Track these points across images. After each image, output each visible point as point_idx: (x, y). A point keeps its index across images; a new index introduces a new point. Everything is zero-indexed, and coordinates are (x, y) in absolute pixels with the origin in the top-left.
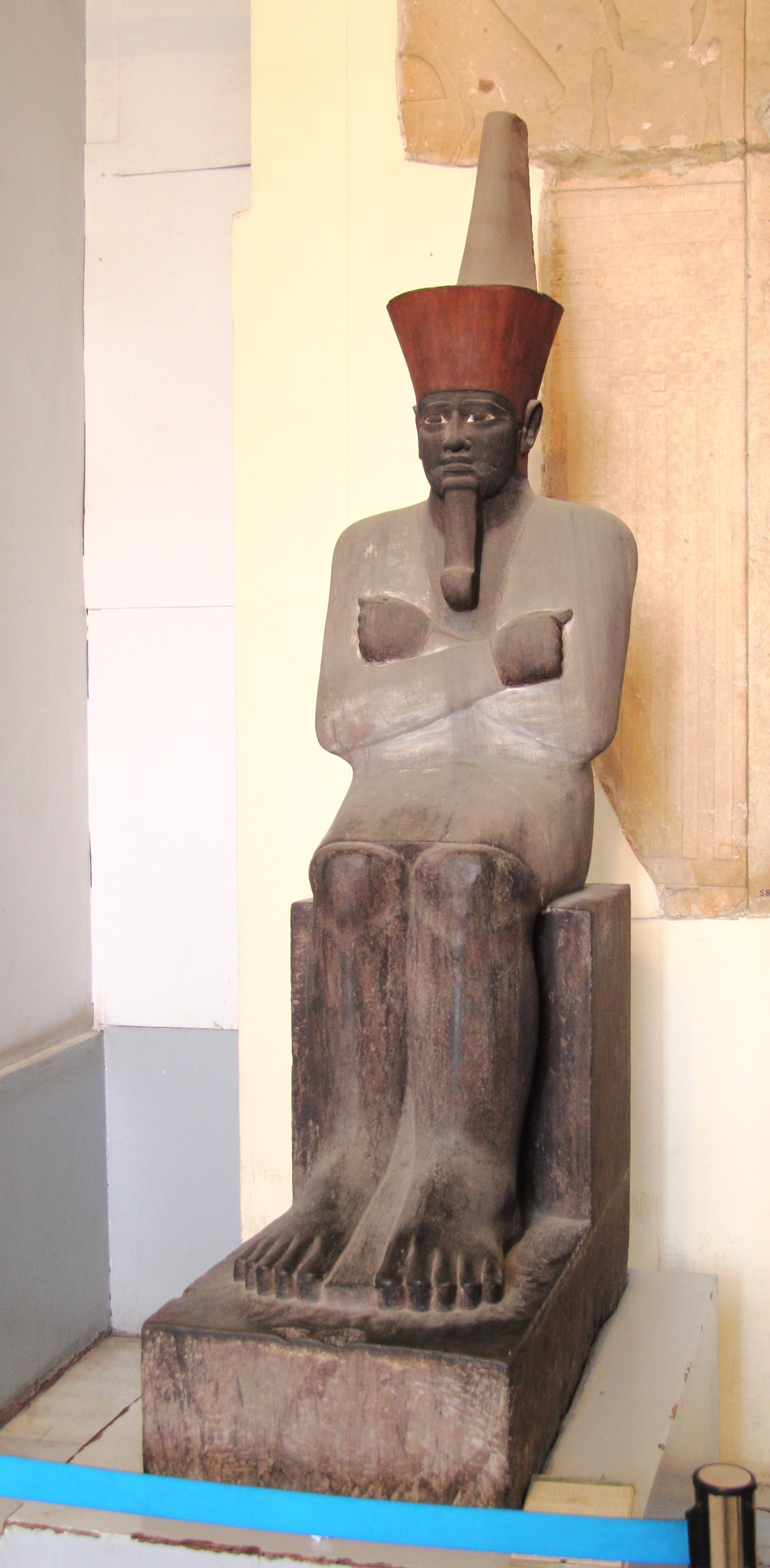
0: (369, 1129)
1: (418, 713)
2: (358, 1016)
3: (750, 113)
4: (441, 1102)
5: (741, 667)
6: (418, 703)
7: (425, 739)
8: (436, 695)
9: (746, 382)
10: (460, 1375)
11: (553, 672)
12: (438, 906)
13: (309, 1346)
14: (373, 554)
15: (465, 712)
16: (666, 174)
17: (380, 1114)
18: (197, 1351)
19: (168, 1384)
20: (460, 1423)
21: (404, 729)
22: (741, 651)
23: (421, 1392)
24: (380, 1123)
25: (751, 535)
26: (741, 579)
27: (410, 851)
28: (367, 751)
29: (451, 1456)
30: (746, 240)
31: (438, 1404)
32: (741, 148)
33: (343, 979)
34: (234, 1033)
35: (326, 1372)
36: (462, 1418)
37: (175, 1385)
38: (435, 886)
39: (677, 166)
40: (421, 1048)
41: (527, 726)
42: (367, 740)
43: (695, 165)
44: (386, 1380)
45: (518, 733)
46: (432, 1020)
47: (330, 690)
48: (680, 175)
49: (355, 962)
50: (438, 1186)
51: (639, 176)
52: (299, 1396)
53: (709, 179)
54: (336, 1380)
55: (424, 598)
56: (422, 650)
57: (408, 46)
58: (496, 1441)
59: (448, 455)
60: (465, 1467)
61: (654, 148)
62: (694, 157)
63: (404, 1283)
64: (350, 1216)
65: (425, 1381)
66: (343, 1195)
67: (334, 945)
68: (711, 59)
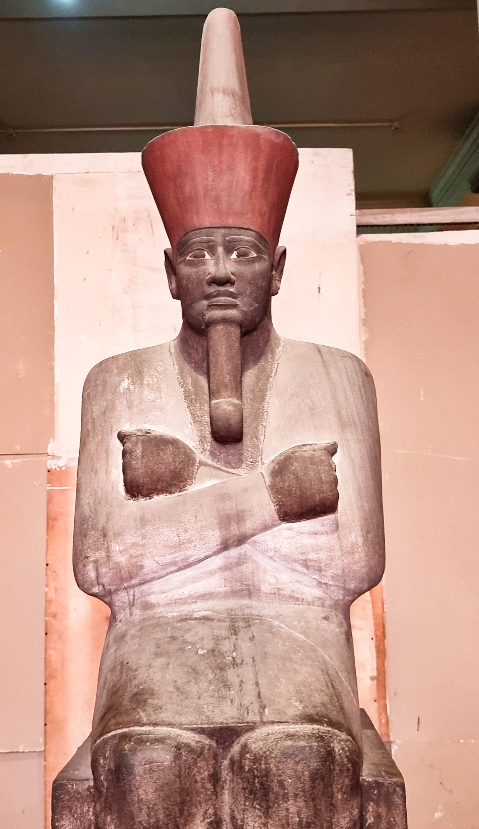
1: (190, 552)
6: (190, 541)
12: (267, 812)
14: (128, 389)
15: (239, 548)
21: (173, 569)
27: (224, 735)
38: (262, 784)
42: (134, 582)
55: (187, 432)
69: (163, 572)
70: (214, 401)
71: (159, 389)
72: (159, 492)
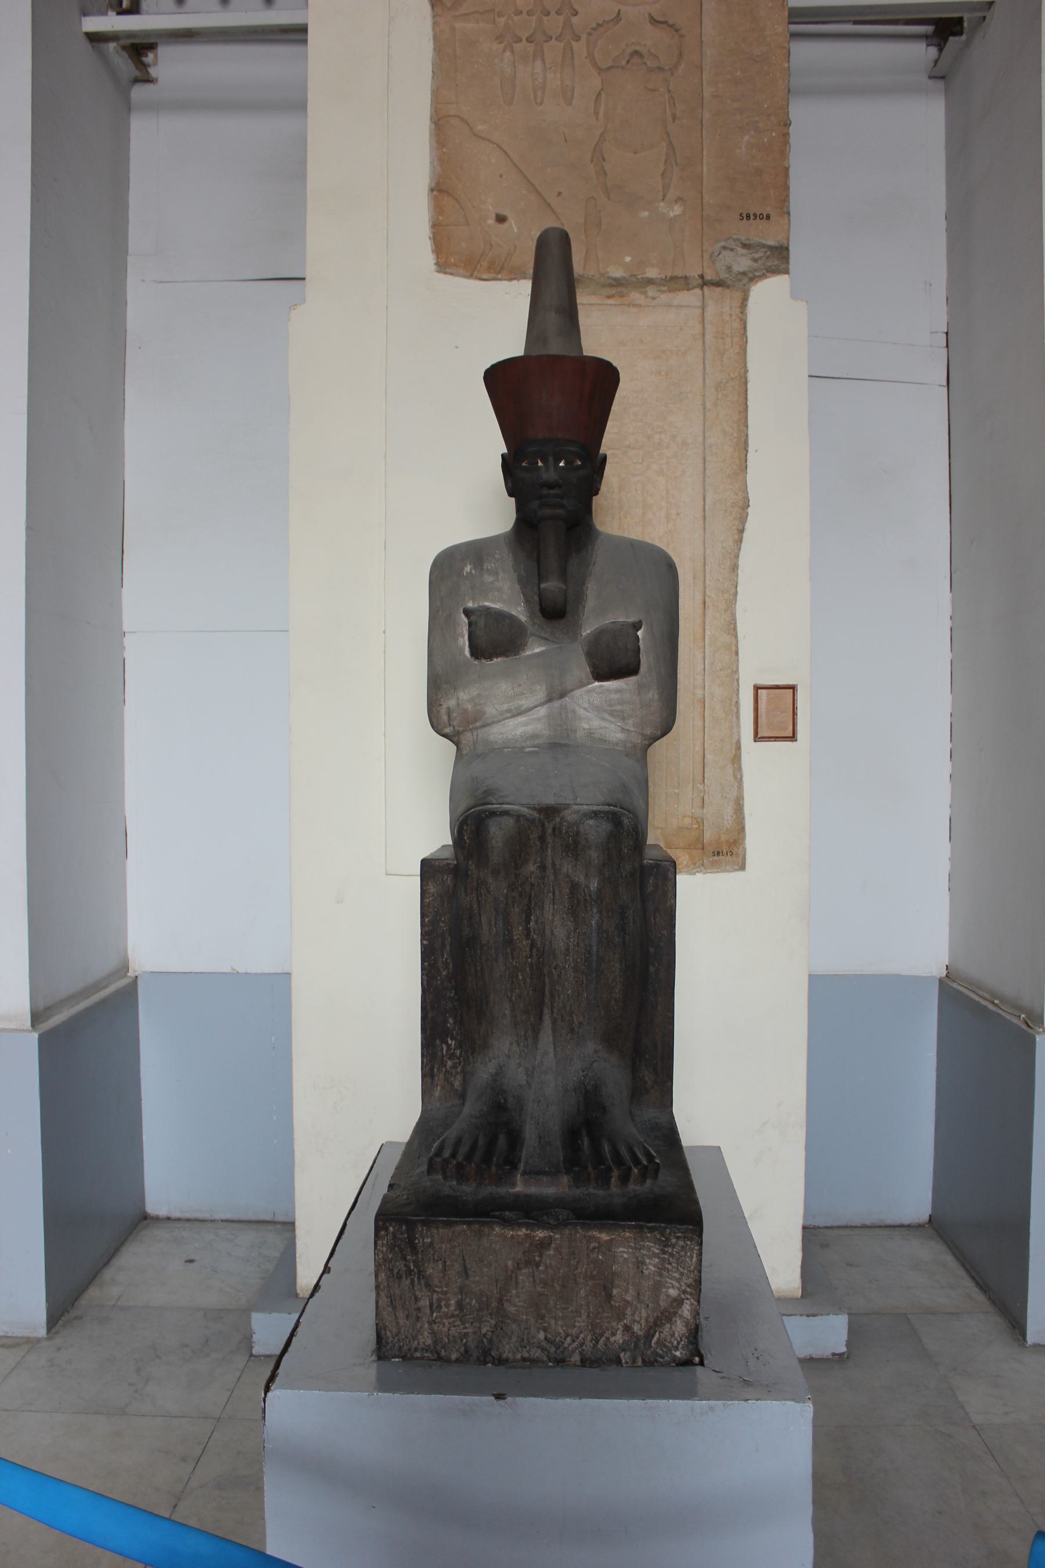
0: (518, 1044)
1: (522, 702)
2: (509, 951)
3: (706, 256)
4: (581, 1019)
5: (699, 678)
7: (526, 724)
8: (539, 687)
9: (704, 459)
10: (660, 1240)
11: (630, 669)
13: (527, 1226)
16: (643, 297)
17: (526, 1031)
18: (425, 1237)
19: (400, 1265)
20: (658, 1278)
22: (700, 667)
23: (625, 1256)
24: (526, 1039)
25: (707, 577)
26: (700, 611)
27: (549, 812)
28: (475, 733)
29: (651, 1305)
30: (704, 351)
31: (640, 1264)
32: (700, 281)
33: (496, 920)
34: (289, 974)
35: (543, 1245)
36: (661, 1275)
37: (405, 1265)
38: (574, 841)
39: (651, 291)
40: (559, 976)
41: (612, 713)
43: (663, 292)
44: (594, 1248)
45: (603, 719)
46: (571, 953)
47: (438, 685)
48: (654, 298)
49: (507, 903)
50: (589, 1087)
51: (622, 296)
52: (519, 1269)
53: (676, 303)
54: (552, 1252)
56: (523, 650)
57: (438, 184)
58: (689, 1290)
59: (545, 491)
60: (662, 1313)
61: (633, 276)
62: (664, 285)
63: (590, 1169)
64: (520, 1115)
65: (630, 1247)
66: (510, 1099)
67: (489, 891)
68: (678, 213)
69: (501, 718)
70: (543, 586)
71: (497, 574)
72: (497, 656)
